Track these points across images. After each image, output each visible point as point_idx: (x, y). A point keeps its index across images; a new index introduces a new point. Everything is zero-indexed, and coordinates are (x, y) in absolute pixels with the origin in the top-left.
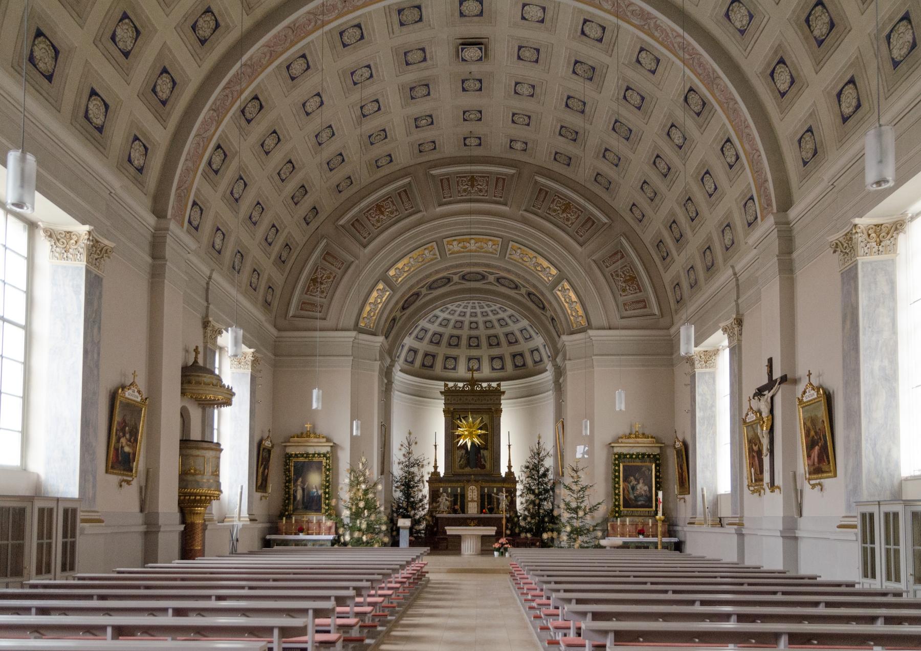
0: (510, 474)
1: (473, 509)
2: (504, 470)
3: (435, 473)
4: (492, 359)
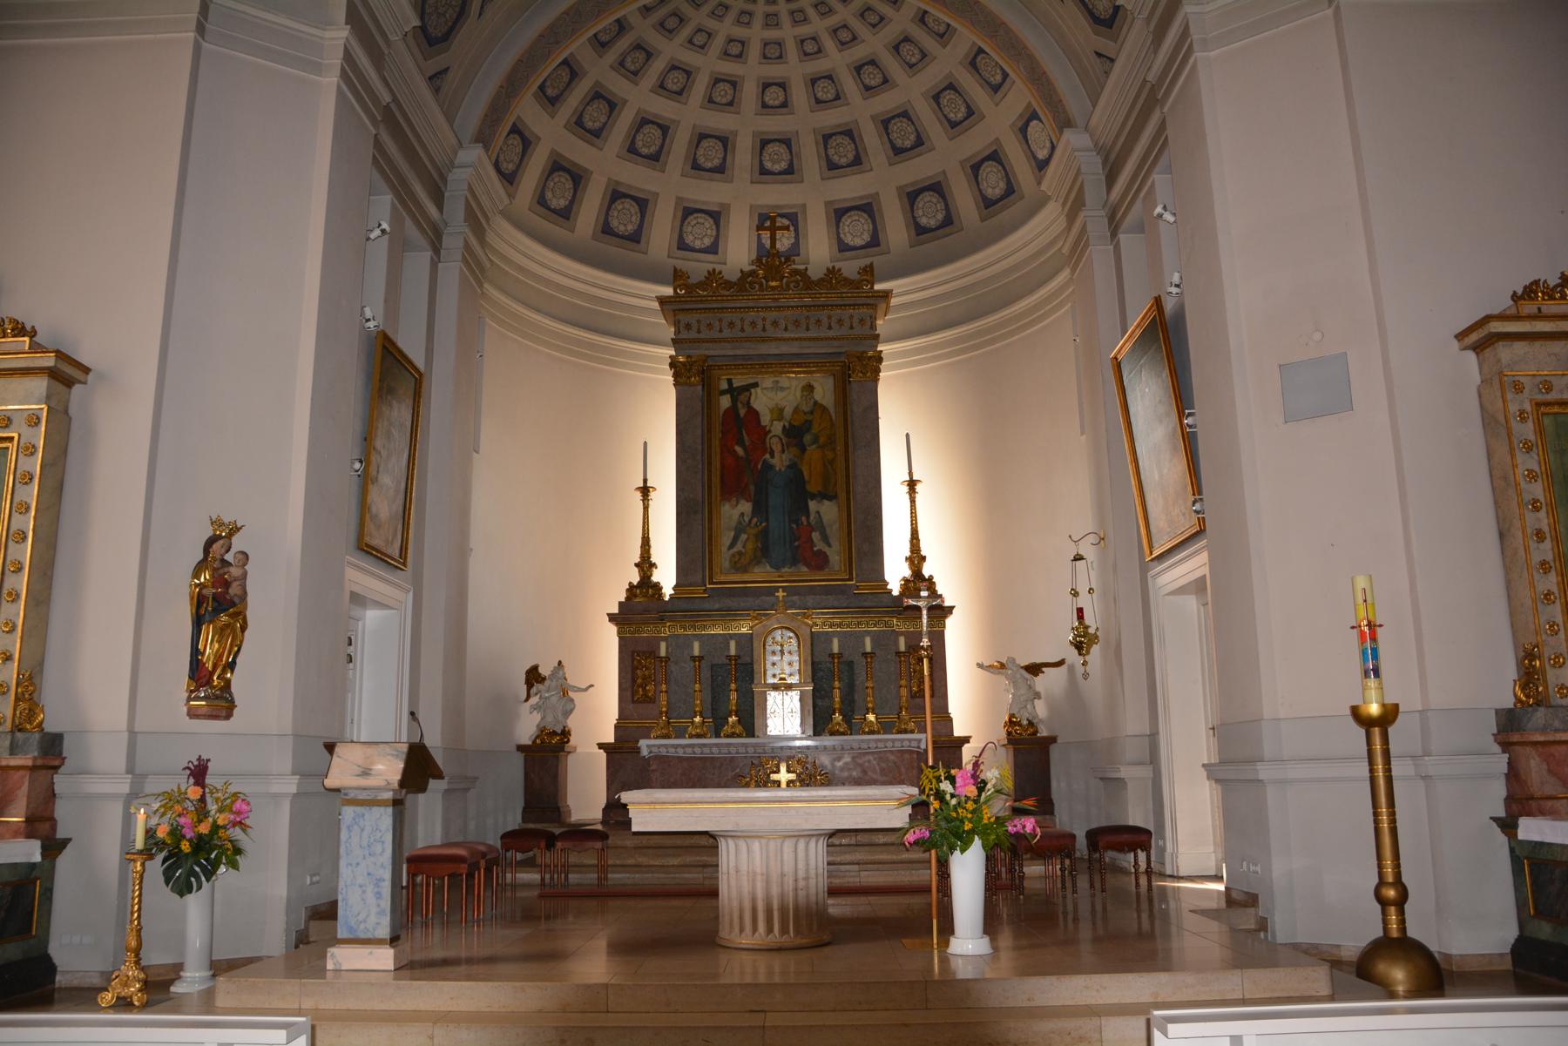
0: (918, 580)
1: (784, 716)
2: (895, 572)
3: (645, 587)
4: (838, 214)
